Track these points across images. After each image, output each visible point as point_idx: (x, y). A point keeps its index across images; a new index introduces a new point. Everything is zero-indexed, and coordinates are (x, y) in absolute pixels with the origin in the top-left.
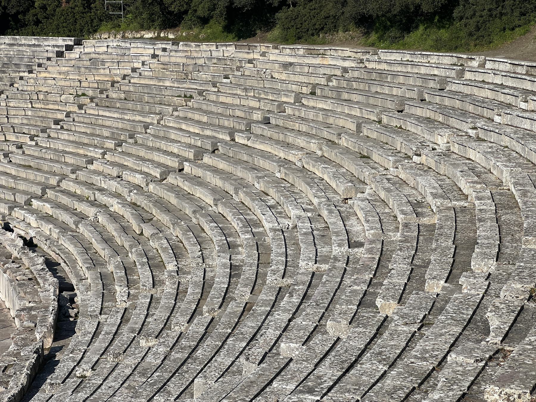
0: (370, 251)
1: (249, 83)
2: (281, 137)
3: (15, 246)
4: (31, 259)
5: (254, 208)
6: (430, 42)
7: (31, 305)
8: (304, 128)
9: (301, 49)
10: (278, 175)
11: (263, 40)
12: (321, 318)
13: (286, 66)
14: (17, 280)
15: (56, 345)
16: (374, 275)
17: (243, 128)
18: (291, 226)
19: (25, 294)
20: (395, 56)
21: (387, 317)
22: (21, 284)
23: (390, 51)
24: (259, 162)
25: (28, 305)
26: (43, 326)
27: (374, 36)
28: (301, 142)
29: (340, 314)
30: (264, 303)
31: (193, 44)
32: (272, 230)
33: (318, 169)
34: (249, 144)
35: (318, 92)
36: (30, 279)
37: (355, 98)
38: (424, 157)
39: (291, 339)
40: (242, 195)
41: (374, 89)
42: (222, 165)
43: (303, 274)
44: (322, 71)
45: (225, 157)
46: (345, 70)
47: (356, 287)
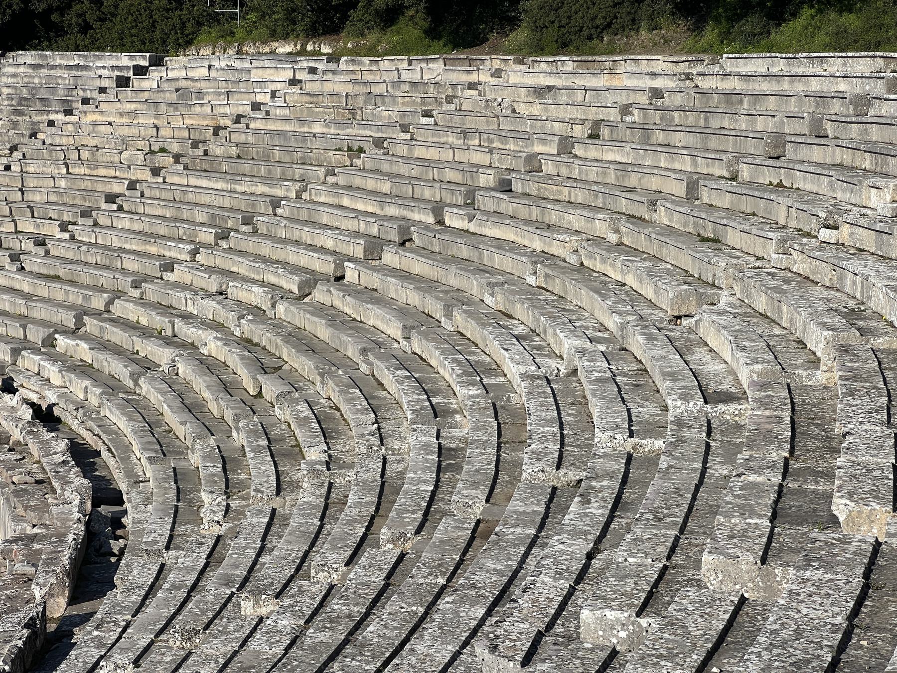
0: (765, 403)
1: (470, 123)
2: (535, 213)
3: (16, 420)
4: (44, 443)
5: (484, 340)
6: (822, 38)
7: (36, 530)
8: (579, 196)
9: (568, 63)
10: (531, 280)
11: (496, 50)
12: (672, 550)
13: (540, 92)
14: (13, 483)
15: (75, 610)
16: (792, 452)
17: (460, 201)
18: (563, 371)
19: (25, 511)
20: (755, 65)
21: (877, 545)
22: (19, 491)
23: (745, 55)
24: (492, 259)
25: (30, 531)
26: (49, 572)
27: (710, 34)
28: (574, 220)
29: (731, 537)
30: (521, 519)
31: (365, 60)
32: (525, 376)
33: (613, 266)
34: (472, 227)
35: (605, 132)
36: (38, 482)
37: (678, 139)
38: (845, 229)
39: (606, 599)
40: (459, 317)
41: (715, 123)
42: (419, 266)
43: (605, 456)
44: (610, 98)
45: (424, 252)
46: (657, 93)
47: (753, 478)
